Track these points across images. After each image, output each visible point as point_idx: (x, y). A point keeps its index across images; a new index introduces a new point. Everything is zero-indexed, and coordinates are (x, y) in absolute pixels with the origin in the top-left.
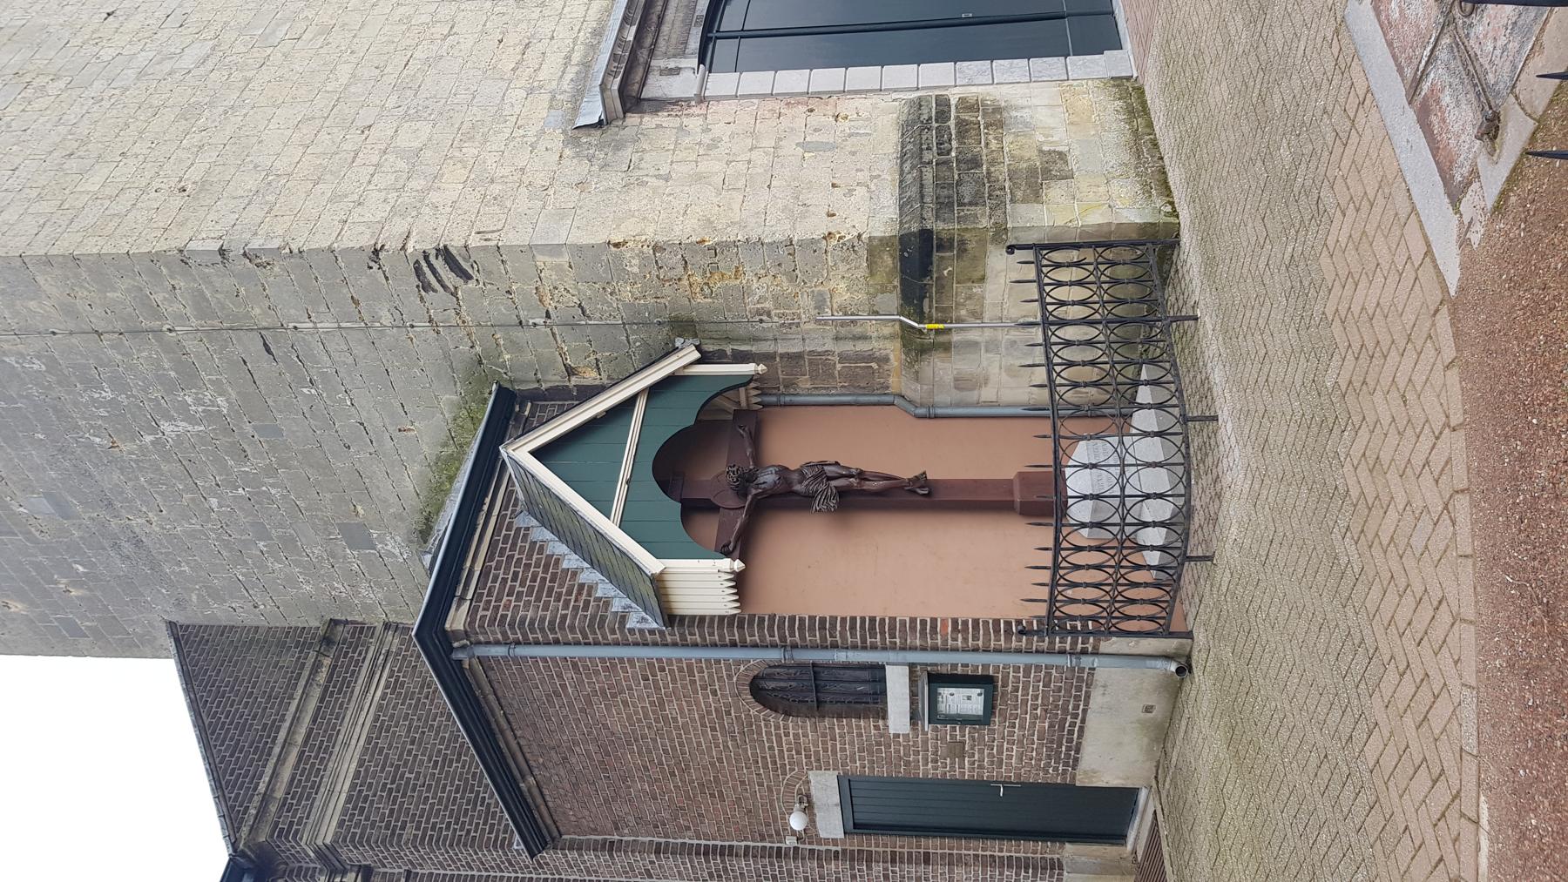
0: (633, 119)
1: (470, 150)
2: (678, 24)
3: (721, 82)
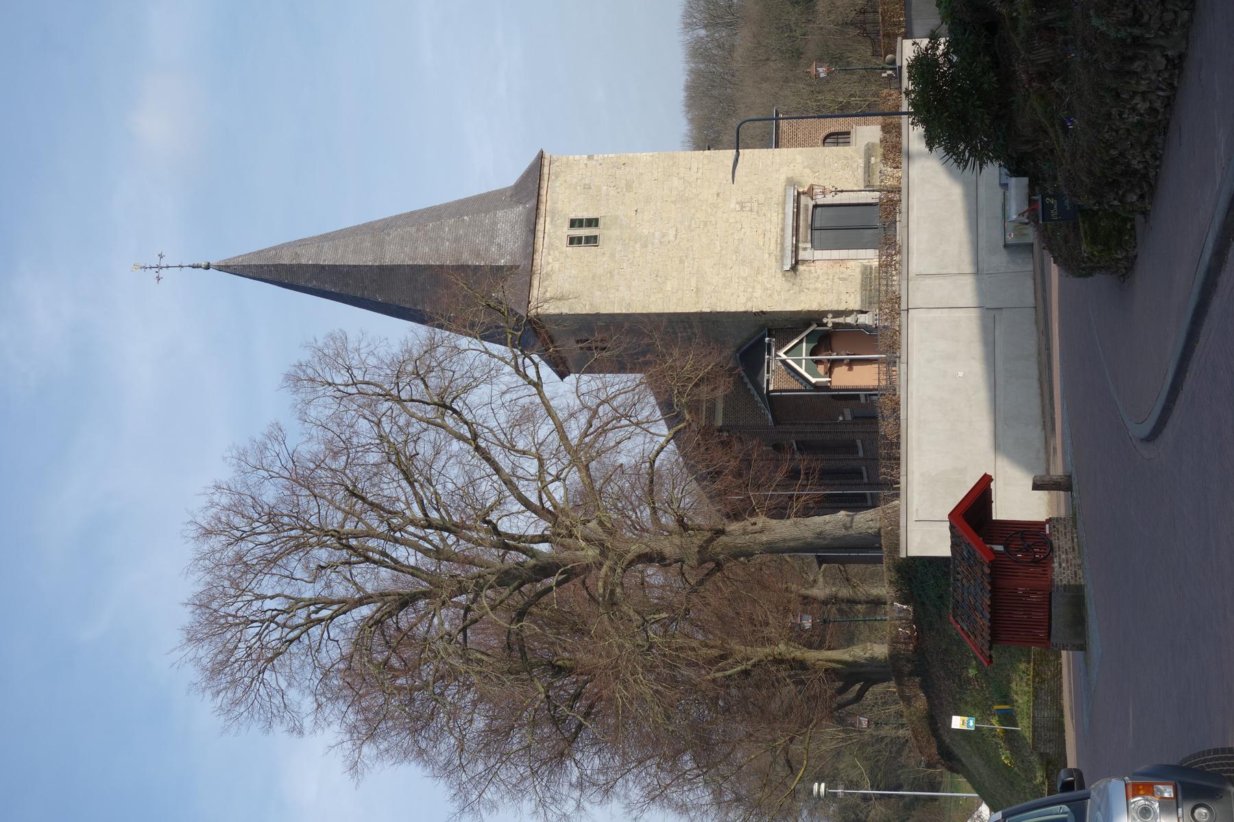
1: (760, 278)
3: (819, 254)
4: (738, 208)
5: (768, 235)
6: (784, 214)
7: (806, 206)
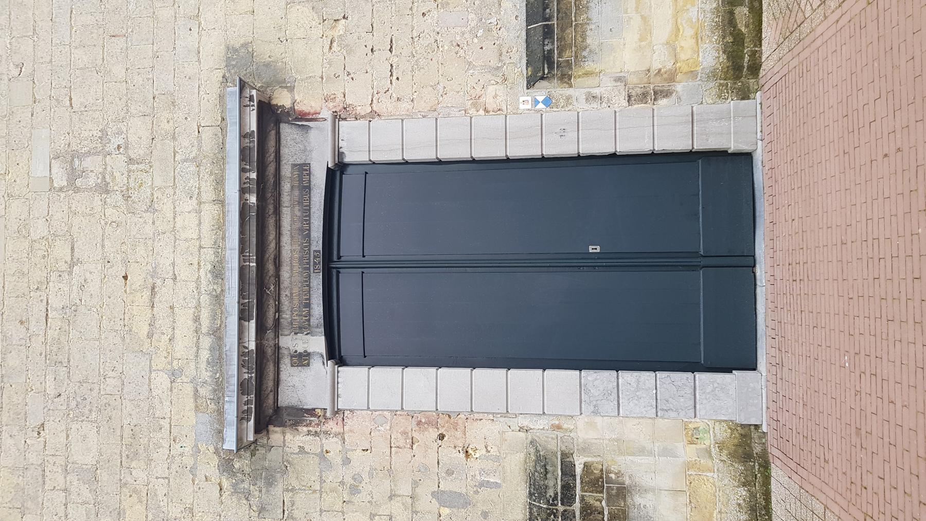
0: (276, 435)
2: (296, 264)
4: (60, 180)
5: (165, 293)
6: (221, 202)
7: (304, 169)
